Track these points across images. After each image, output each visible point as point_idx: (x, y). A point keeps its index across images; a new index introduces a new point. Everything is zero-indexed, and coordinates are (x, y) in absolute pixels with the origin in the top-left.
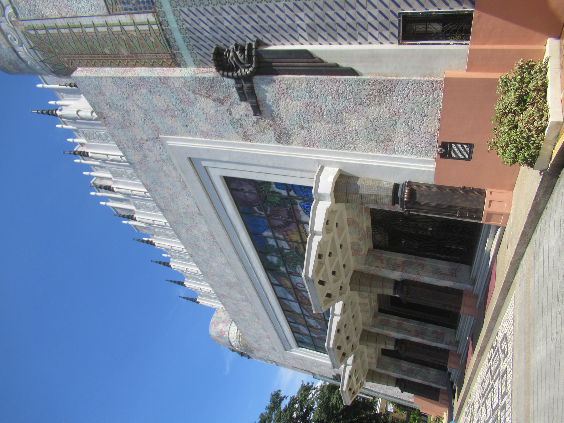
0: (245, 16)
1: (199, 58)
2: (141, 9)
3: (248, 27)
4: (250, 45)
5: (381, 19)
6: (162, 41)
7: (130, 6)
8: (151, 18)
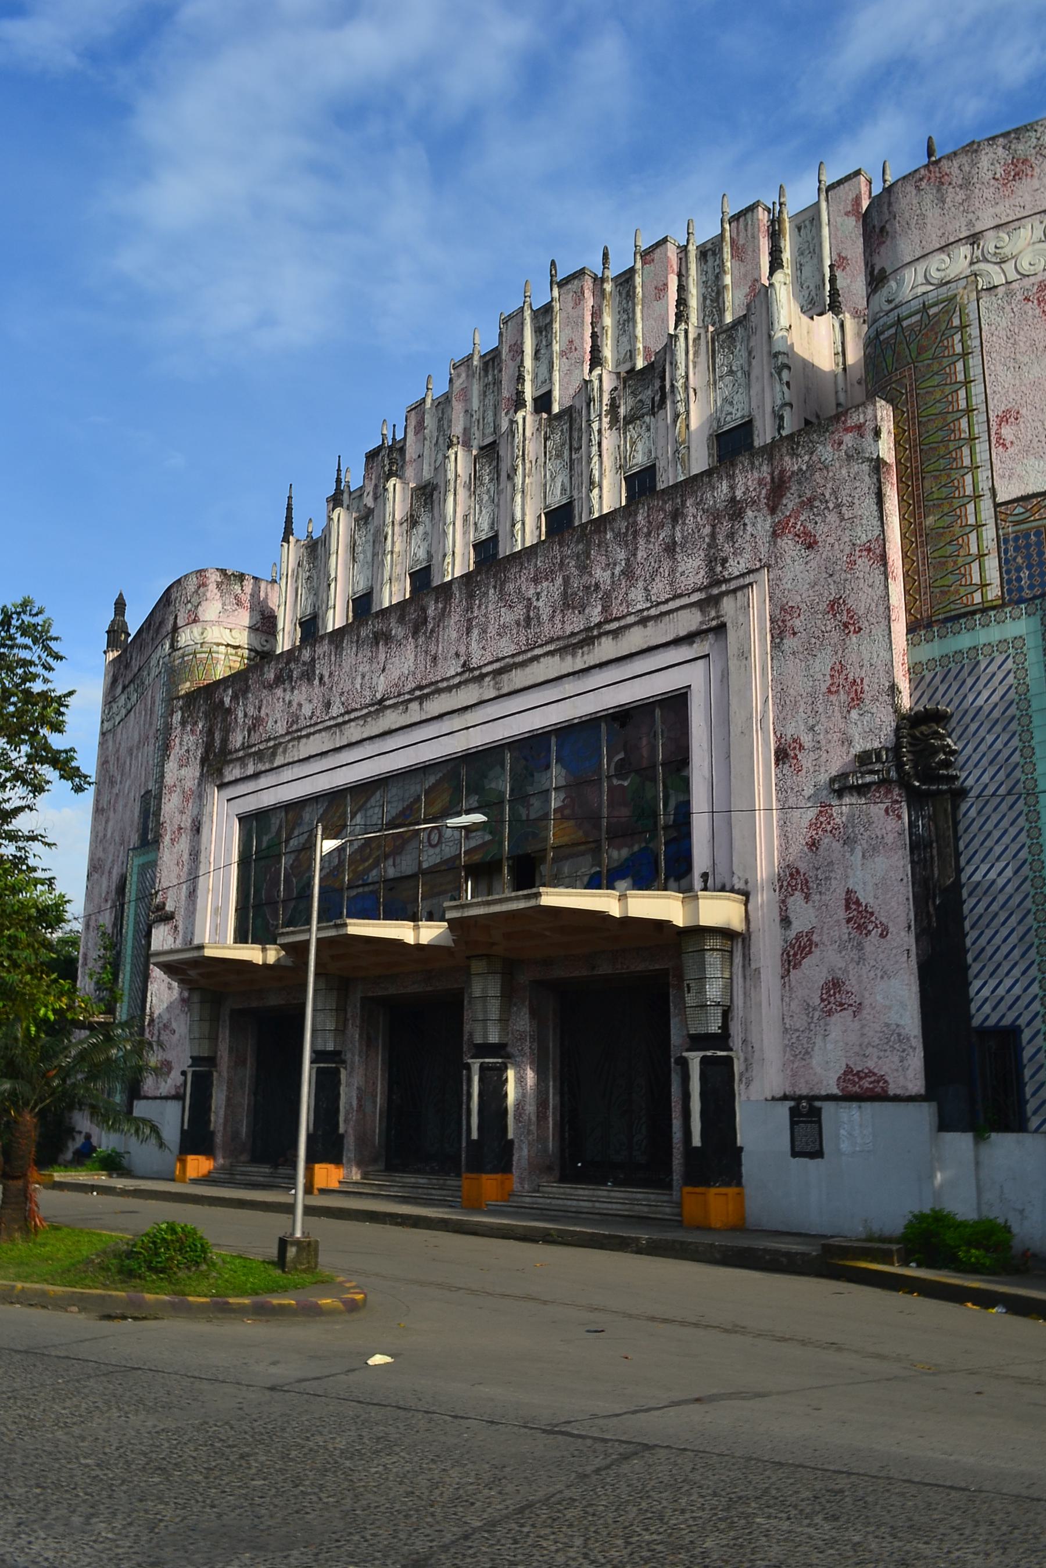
0: (1002, 774)
1: (929, 676)
2: (1008, 572)
3: (986, 778)
4: (957, 777)
5: (1009, 1000)
6: (953, 606)
7: (1011, 552)
8: (994, 592)
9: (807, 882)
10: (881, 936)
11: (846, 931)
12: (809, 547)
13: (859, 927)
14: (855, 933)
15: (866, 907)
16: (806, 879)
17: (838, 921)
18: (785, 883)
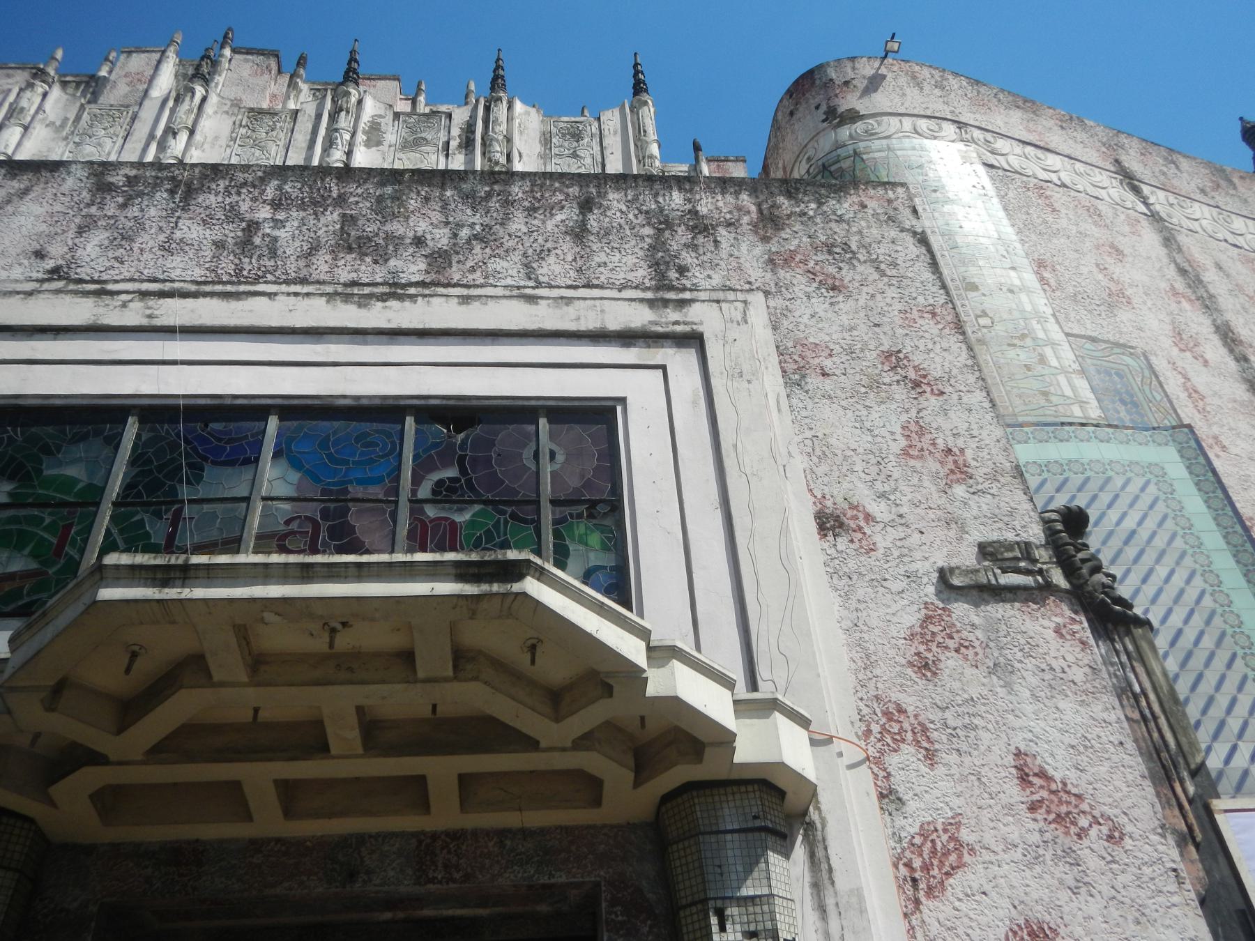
0: (1198, 621)
9: (925, 730)
10: (1110, 837)
11: (1032, 825)
12: (834, 288)
13: (1059, 818)
14: (1052, 831)
15: (1065, 784)
16: (920, 724)
17: (1010, 807)
18: (875, 728)
